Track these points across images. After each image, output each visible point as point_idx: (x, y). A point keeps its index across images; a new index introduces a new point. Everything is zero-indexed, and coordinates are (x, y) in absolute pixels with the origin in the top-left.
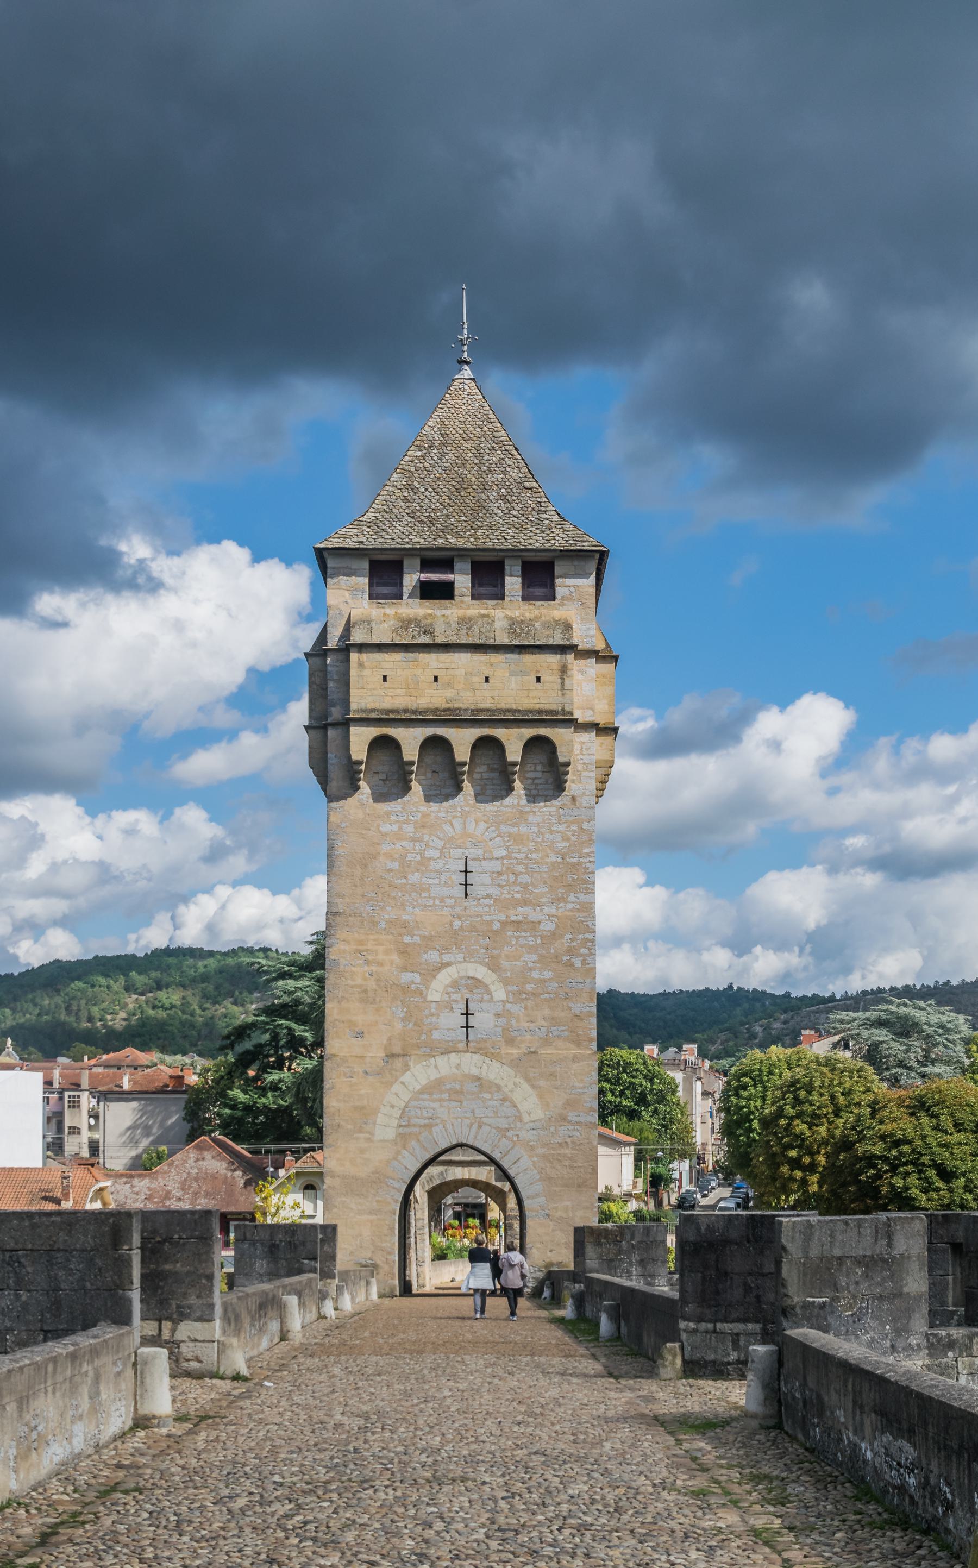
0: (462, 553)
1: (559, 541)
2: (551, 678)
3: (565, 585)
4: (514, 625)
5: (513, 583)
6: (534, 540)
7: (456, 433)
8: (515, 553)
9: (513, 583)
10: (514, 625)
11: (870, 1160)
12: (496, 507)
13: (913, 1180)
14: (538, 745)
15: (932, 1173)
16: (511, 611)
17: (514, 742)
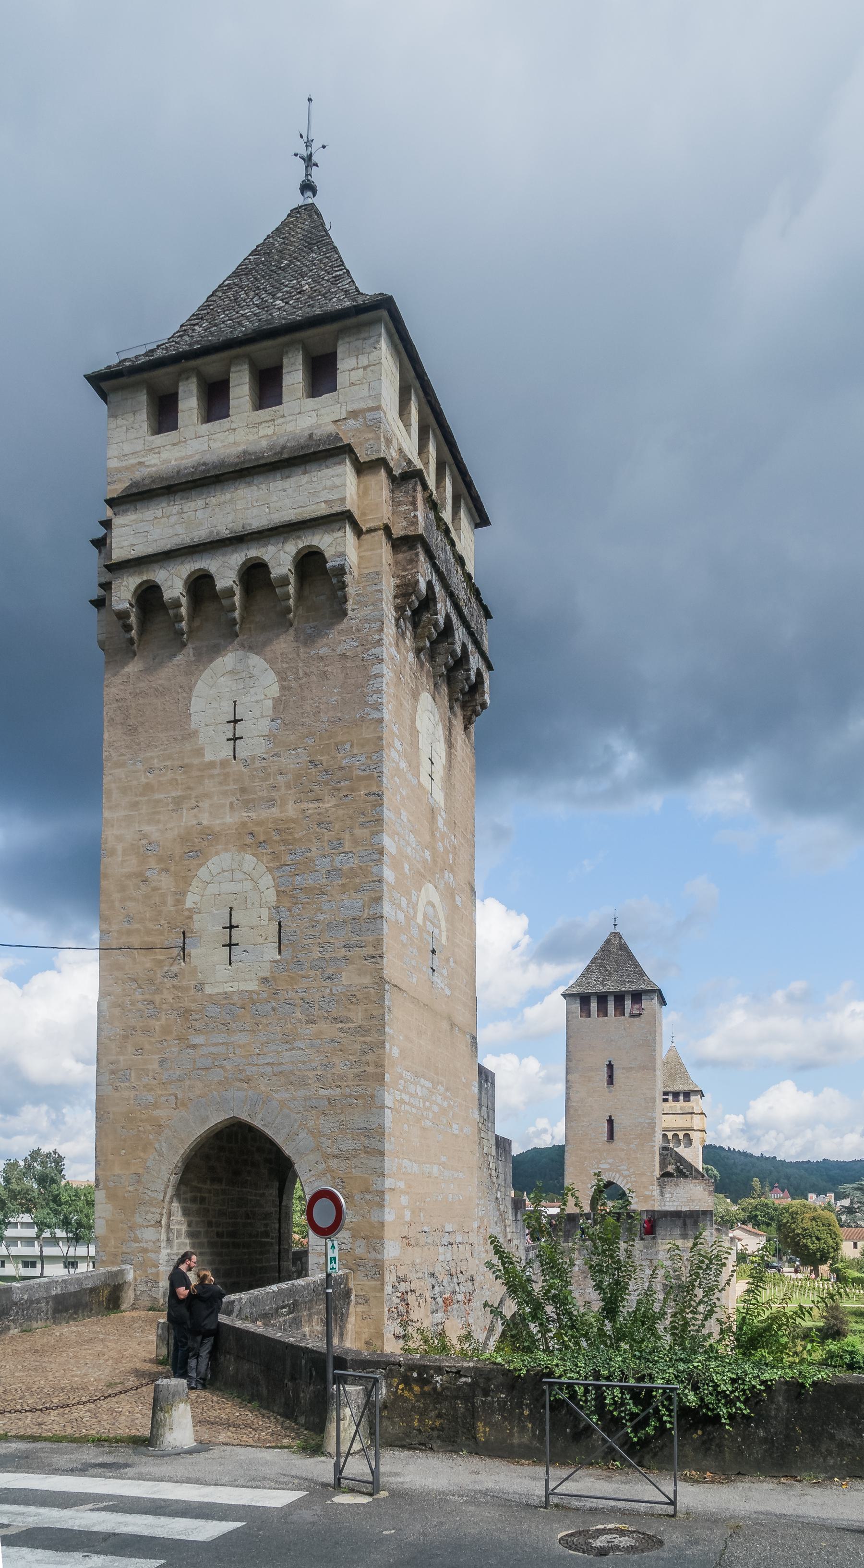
0: (670, 1092)
1: (691, 1089)
2: (689, 1120)
3: (692, 1098)
4: (681, 1108)
5: (681, 1098)
6: (686, 1088)
7: (670, 1061)
8: (681, 1091)
9: (681, 1098)
10: (681, 1108)
11: (798, 1235)
12: (678, 1079)
13: (809, 1240)
14: (687, 1135)
15: (814, 1238)
16: (681, 1104)
17: (681, 1135)
